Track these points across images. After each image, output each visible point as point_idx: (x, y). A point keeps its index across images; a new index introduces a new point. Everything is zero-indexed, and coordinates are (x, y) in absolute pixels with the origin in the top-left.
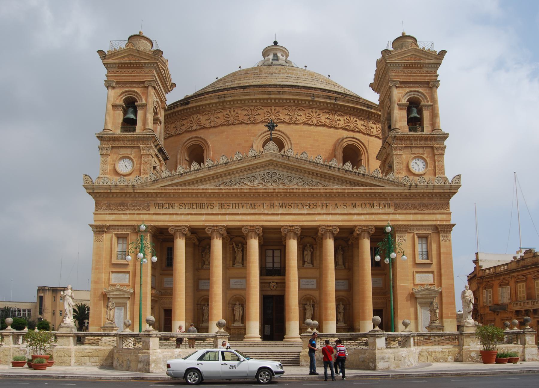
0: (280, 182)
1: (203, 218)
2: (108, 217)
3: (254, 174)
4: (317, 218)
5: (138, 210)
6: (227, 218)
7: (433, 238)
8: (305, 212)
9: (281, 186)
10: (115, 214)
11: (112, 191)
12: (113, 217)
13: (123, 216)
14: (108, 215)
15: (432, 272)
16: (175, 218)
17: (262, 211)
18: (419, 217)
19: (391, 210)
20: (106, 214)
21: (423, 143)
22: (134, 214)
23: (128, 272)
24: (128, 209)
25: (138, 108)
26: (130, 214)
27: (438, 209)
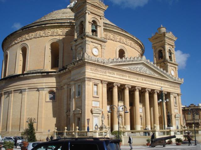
0: (144, 71)
1: (124, 81)
2: (92, 74)
3: (137, 66)
4: (154, 86)
5: (103, 73)
6: (131, 82)
7: (177, 97)
8: (151, 83)
9: (145, 72)
10: (94, 73)
11: (96, 63)
12: (93, 75)
13: (97, 74)
14: (91, 73)
15: (177, 109)
16: (115, 79)
17: (140, 81)
18: (175, 90)
19: (169, 87)
20: (91, 73)
21: (173, 65)
22: (101, 75)
23: (99, 101)
24: (99, 72)
25: (98, 27)
26: (100, 74)
27: (178, 88)
